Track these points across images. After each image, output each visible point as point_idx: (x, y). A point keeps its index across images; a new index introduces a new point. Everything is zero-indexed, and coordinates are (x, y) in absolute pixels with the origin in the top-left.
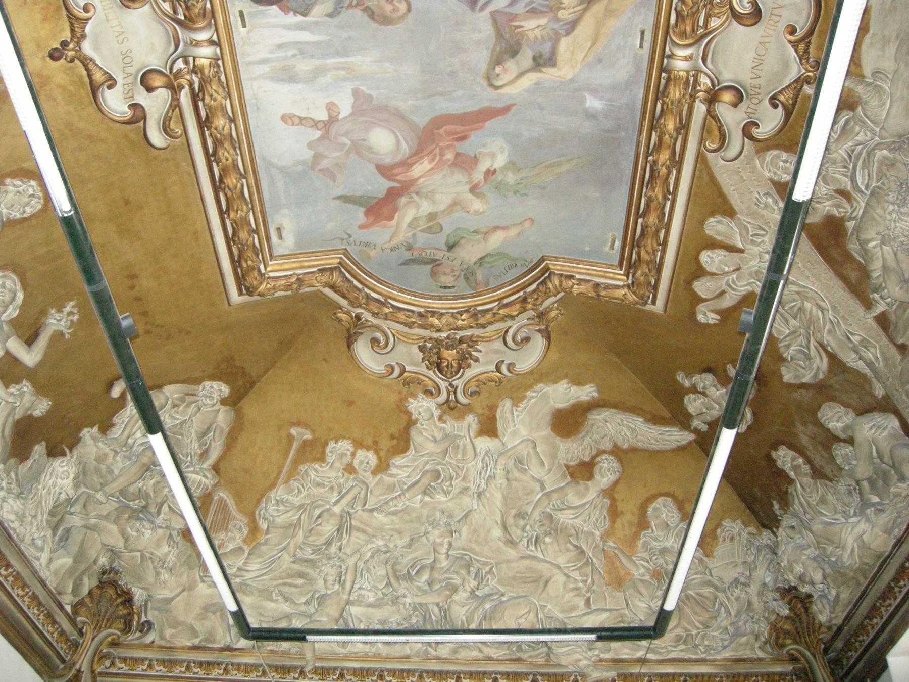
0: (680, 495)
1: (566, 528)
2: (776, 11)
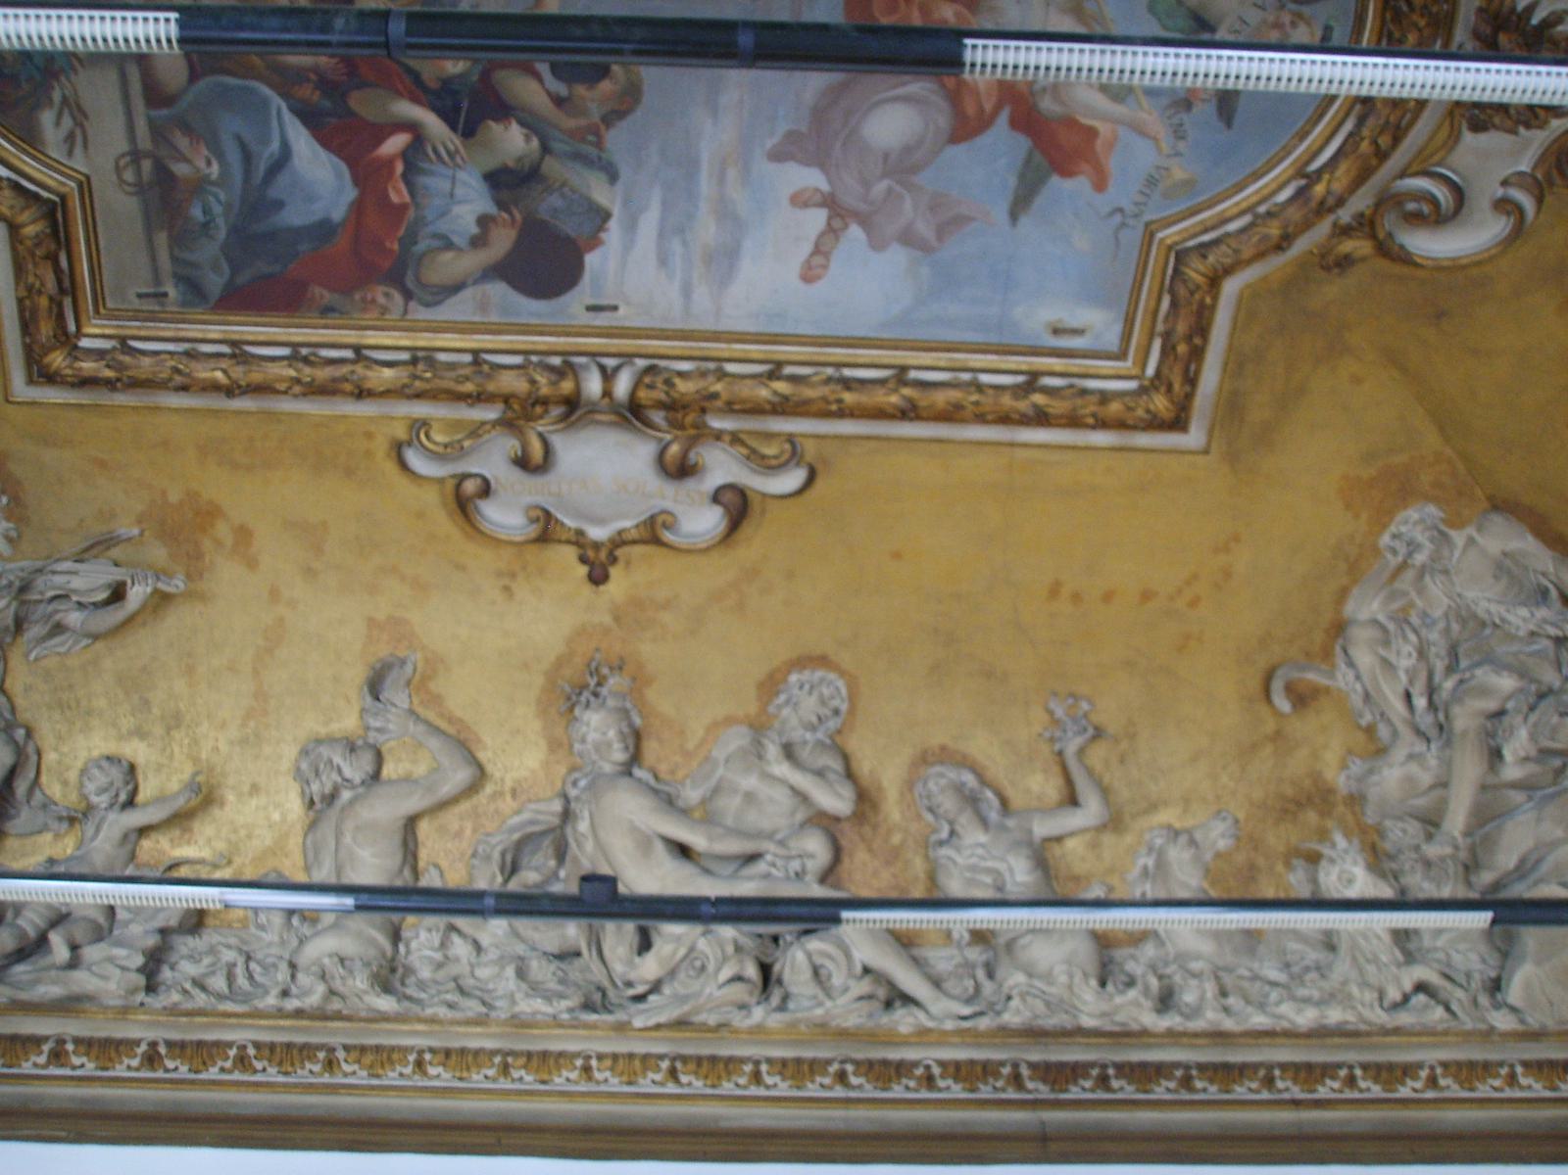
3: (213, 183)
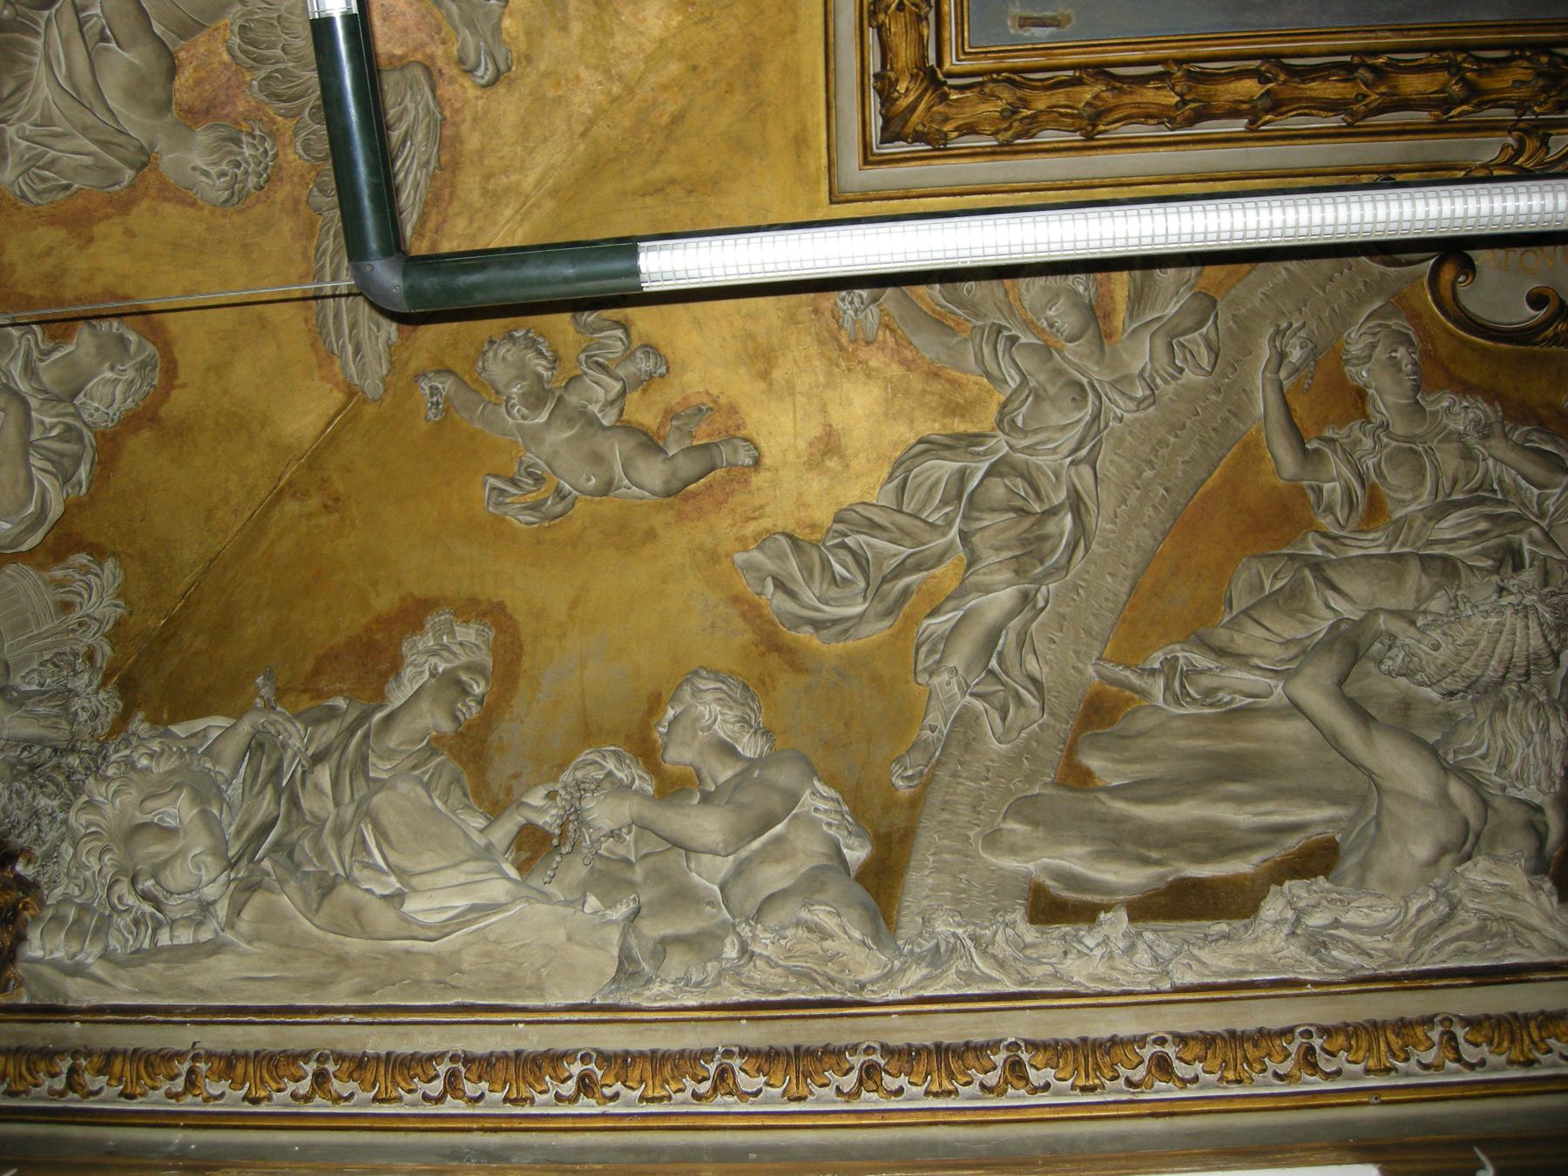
0: (180, 402)
1: (14, 61)
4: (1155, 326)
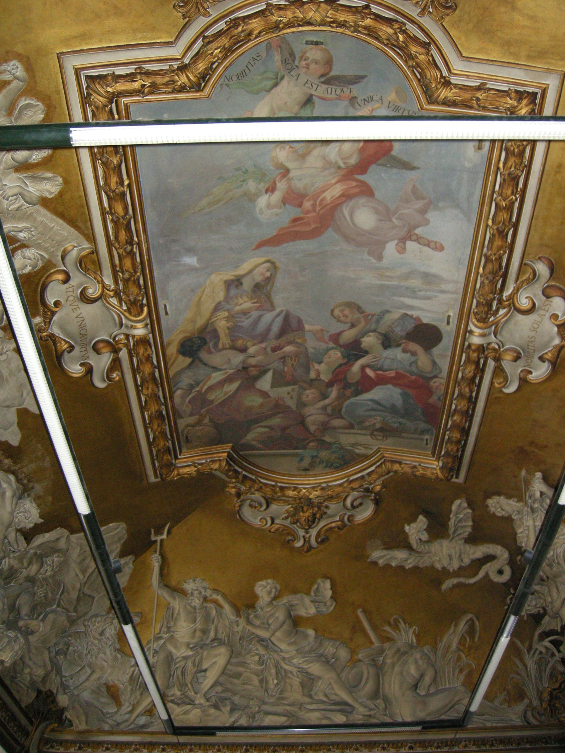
2: (85, 353)
3: (384, 420)
4: (23, 186)
